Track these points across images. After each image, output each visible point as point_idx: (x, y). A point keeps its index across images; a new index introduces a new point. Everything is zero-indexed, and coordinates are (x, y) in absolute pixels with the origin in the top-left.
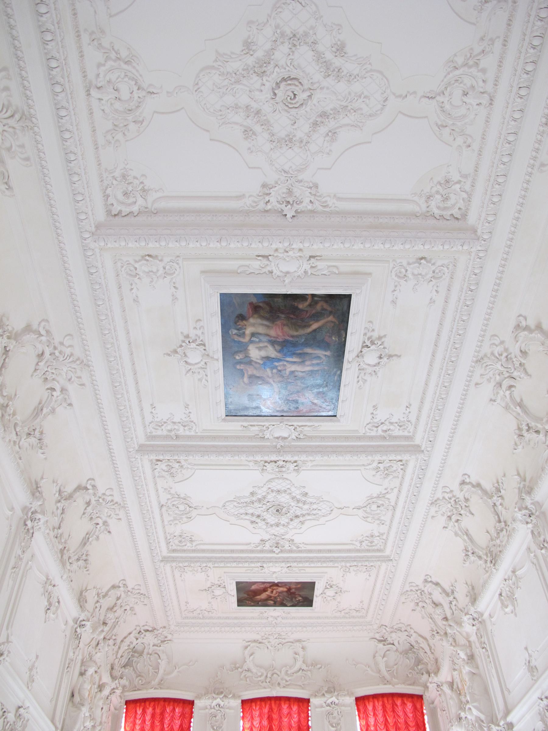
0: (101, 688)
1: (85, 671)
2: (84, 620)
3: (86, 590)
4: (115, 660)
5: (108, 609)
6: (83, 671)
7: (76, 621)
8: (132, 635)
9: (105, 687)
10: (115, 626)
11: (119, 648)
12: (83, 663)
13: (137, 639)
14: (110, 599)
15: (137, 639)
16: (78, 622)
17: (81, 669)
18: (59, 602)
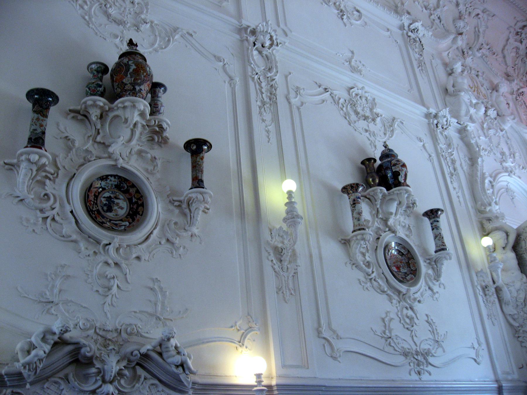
0: (495, 88)
1: (452, 70)
2: (411, 24)
3: (403, 4)
4: (506, 69)
5: (454, 21)
6: (450, 72)
7: (402, 27)
8: (511, 41)
9: (498, 86)
10: (478, 36)
11: (504, 57)
12: (446, 65)
13: (521, 42)
14: (445, 8)
15: (521, 42)
16: (406, 28)
17: (447, 71)
18: (358, 11)
